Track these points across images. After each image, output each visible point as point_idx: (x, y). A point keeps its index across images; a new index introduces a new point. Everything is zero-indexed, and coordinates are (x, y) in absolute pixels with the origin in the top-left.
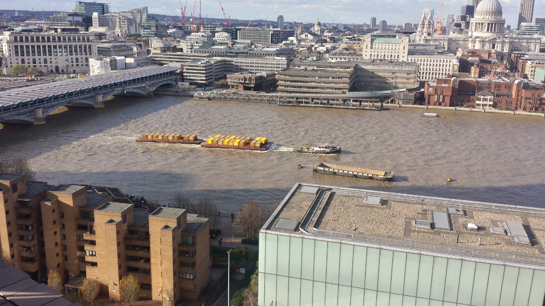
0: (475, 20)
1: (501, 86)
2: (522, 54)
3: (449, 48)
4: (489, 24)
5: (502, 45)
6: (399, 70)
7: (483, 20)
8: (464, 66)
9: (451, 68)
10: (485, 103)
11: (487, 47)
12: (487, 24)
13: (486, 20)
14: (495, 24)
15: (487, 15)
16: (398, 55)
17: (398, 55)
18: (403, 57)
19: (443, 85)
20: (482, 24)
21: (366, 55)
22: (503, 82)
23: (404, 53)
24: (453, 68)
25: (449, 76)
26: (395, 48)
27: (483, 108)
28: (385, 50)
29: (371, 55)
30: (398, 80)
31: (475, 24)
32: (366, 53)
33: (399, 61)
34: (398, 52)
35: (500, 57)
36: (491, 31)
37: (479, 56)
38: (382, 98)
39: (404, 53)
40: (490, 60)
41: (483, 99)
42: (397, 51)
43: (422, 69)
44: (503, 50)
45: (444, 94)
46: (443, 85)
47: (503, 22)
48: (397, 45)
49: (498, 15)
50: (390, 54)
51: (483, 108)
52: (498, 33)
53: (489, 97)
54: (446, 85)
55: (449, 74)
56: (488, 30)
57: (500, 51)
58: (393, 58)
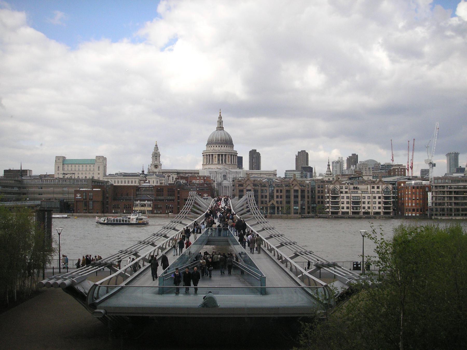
1: (163, 189)
4: (219, 155)
7: (212, 151)
10: (143, 208)
12: (217, 155)
13: (215, 151)
14: (225, 155)
15: (216, 146)
20: (212, 155)
23: (99, 174)
28: (82, 172)
39: (99, 174)
42: (91, 173)
47: (233, 154)
49: (228, 147)
52: (230, 164)
54: (100, 189)
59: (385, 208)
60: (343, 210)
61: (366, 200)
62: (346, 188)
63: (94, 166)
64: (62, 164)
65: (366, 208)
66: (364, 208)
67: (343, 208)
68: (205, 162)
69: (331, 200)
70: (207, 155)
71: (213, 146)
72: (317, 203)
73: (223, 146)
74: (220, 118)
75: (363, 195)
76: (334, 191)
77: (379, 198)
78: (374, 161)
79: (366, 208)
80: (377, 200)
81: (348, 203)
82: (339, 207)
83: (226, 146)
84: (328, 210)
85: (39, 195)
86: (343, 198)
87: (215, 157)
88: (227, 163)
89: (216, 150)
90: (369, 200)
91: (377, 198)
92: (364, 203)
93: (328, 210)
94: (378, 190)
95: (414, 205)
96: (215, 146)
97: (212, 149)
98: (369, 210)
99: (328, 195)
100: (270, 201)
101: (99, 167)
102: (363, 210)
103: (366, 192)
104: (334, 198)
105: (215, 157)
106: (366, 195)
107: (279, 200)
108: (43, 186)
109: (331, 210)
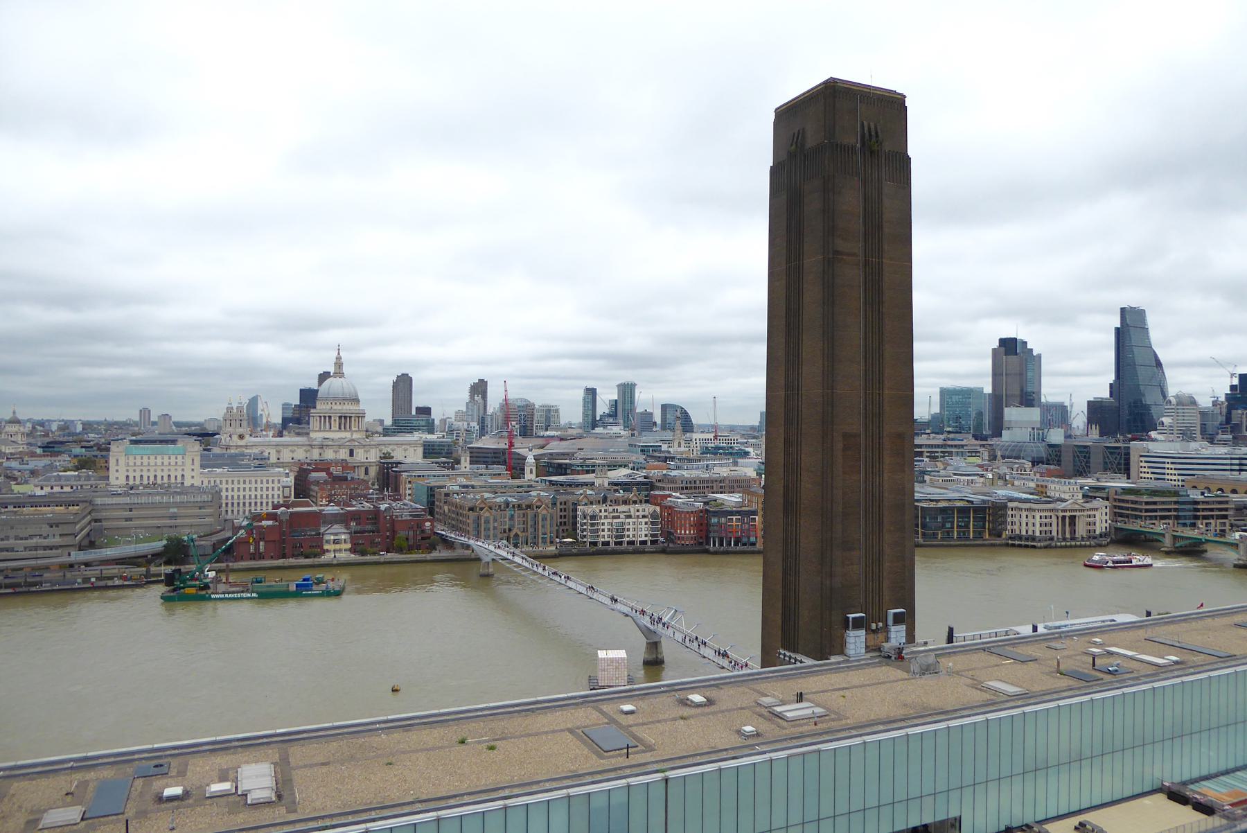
0: (318, 411)
2: (395, 463)
3: (278, 459)
4: (340, 417)
5: (365, 451)
6: (183, 502)
8: (302, 488)
9: (280, 493)
11: (343, 454)
15: (336, 403)
16: (183, 476)
17: (183, 476)
18: (193, 477)
19: (264, 523)
21: (117, 478)
22: (363, 509)
23: (193, 470)
24: (283, 491)
25: (276, 507)
26: (176, 463)
27: (335, 556)
29: (127, 477)
30: (179, 521)
31: (318, 418)
32: (117, 475)
33: (185, 485)
34: (183, 470)
35: (363, 469)
36: (345, 428)
37: (327, 470)
38: (149, 556)
39: (193, 470)
40: (345, 475)
41: (334, 540)
43: (224, 497)
44: (367, 458)
45: (266, 539)
46: (264, 523)
47: (361, 415)
48: (180, 457)
50: (165, 475)
51: (335, 556)
53: (343, 537)
54: (270, 523)
55: (278, 502)
56: (340, 428)
57: (362, 461)
58: (173, 480)
59: (652, 536)
60: (603, 540)
61: (631, 527)
62: (606, 511)
63: (183, 458)
64: (124, 454)
65: (631, 536)
66: (628, 536)
67: (603, 536)
68: (317, 427)
69: (589, 527)
70: (321, 417)
71: (329, 403)
72: (559, 524)
73: (346, 404)
74: (339, 358)
75: (627, 520)
76: (593, 517)
77: (646, 523)
78: (525, 400)
79: (631, 536)
80: (644, 526)
81: (609, 530)
82: (598, 536)
83: (350, 404)
84: (585, 540)
85: (126, 521)
86: (603, 524)
87: (335, 420)
88: (353, 429)
89: (335, 410)
90: (634, 527)
91: (644, 523)
92: (628, 530)
93: (585, 540)
94: (643, 514)
95: (687, 532)
96: (333, 403)
97: (329, 406)
98: (634, 539)
99: (585, 521)
100: (510, 530)
101: (193, 460)
102: (628, 539)
103: (630, 517)
104: (592, 525)
105: (335, 420)
106: (631, 521)
107: (522, 526)
108: (133, 506)
109: (589, 540)
